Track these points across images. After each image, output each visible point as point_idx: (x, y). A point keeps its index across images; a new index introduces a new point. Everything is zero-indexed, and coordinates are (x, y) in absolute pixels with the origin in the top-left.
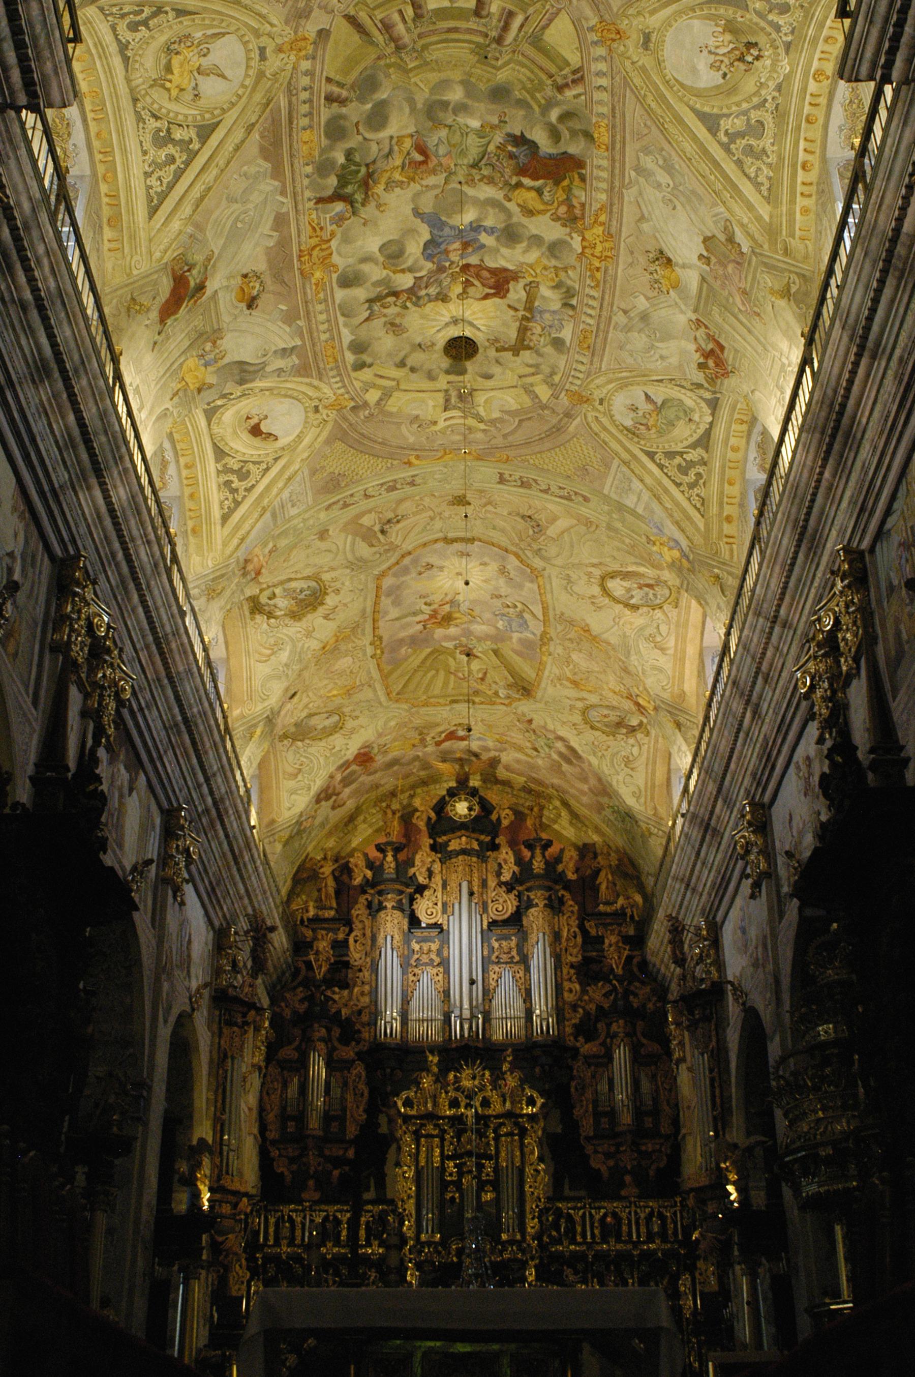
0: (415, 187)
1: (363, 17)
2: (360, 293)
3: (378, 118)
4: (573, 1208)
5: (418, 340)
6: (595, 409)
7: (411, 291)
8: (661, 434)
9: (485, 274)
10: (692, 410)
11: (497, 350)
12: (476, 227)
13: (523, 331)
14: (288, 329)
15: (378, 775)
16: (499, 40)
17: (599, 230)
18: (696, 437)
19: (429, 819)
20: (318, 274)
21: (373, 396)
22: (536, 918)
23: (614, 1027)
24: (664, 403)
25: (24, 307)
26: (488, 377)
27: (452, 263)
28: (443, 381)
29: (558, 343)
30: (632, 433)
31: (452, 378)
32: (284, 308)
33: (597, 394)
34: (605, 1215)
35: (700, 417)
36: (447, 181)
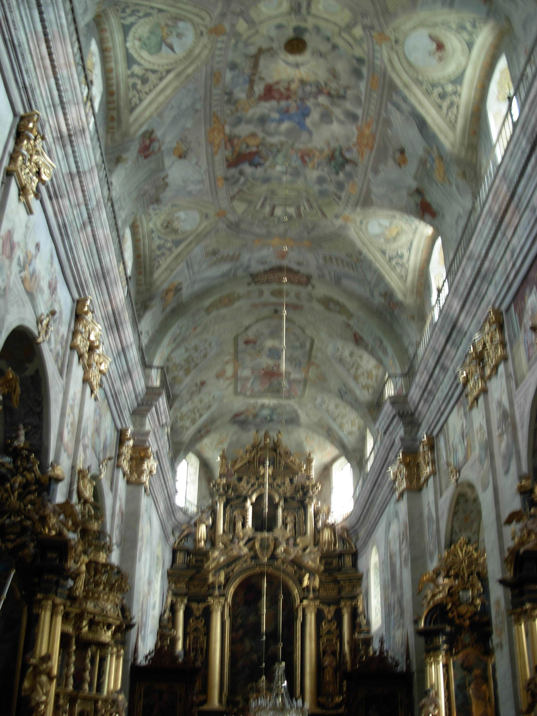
0: (310, 146)
1: (320, 214)
2: (348, 105)
3: (321, 180)
5: (321, 61)
6: (205, 26)
7: (320, 91)
8: (157, 25)
9: (277, 96)
10: (141, 48)
11: (272, 48)
12: (280, 121)
13: (256, 66)
14: (392, 119)
16: (266, 199)
17: (217, 142)
18: (133, 30)
20: (367, 132)
21: (358, 31)
24: (159, 49)
25: (435, 382)
26: (280, 27)
27: (296, 102)
28: (310, 23)
29: (233, 66)
30: (177, 19)
31: (303, 24)
32: (389, 131)
33: (205, 40)
35: (134, 44)
36: (294, 144)
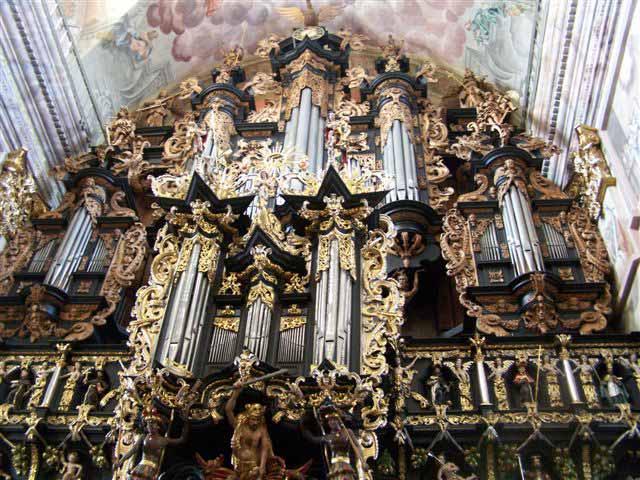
4: (453, 359)
15: (225, 28)
19: (273, 50)
22: (392, 113)
23: (499, 172)
34: (514, 370)
